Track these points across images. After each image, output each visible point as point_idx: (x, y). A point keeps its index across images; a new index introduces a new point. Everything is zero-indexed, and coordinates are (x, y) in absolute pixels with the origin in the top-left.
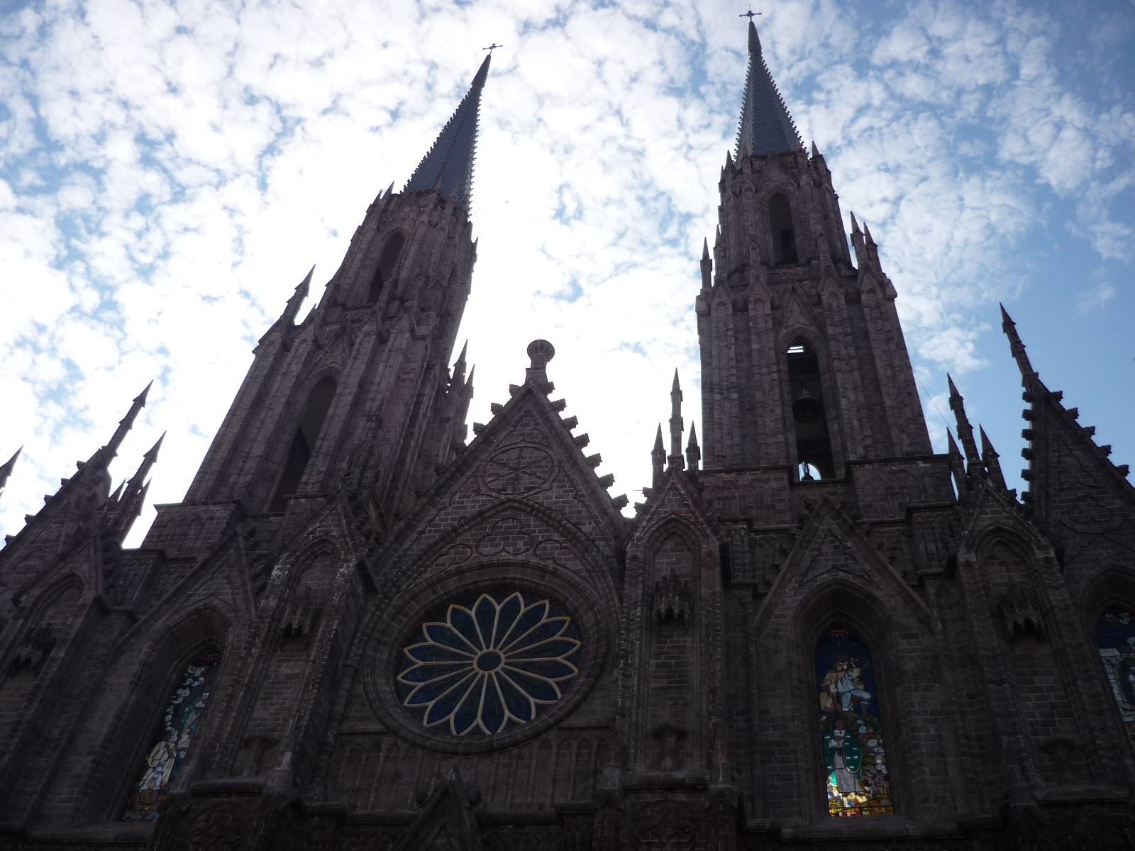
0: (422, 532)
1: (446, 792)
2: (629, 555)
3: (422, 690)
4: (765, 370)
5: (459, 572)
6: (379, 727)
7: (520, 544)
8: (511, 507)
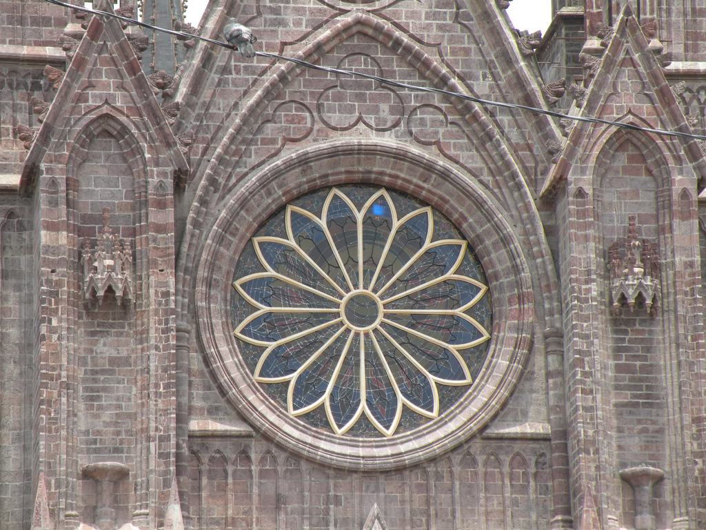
0: (225, 70)
2: (572, 188)
3: (275, 353)
7: (385, 107)
8: (359, 33)
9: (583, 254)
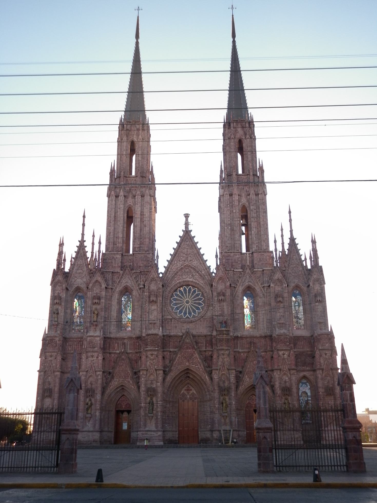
1: (187, 333)
4: (236, 219)
5: (180, 283)
6: (171, 317)
9: (215, 294)
